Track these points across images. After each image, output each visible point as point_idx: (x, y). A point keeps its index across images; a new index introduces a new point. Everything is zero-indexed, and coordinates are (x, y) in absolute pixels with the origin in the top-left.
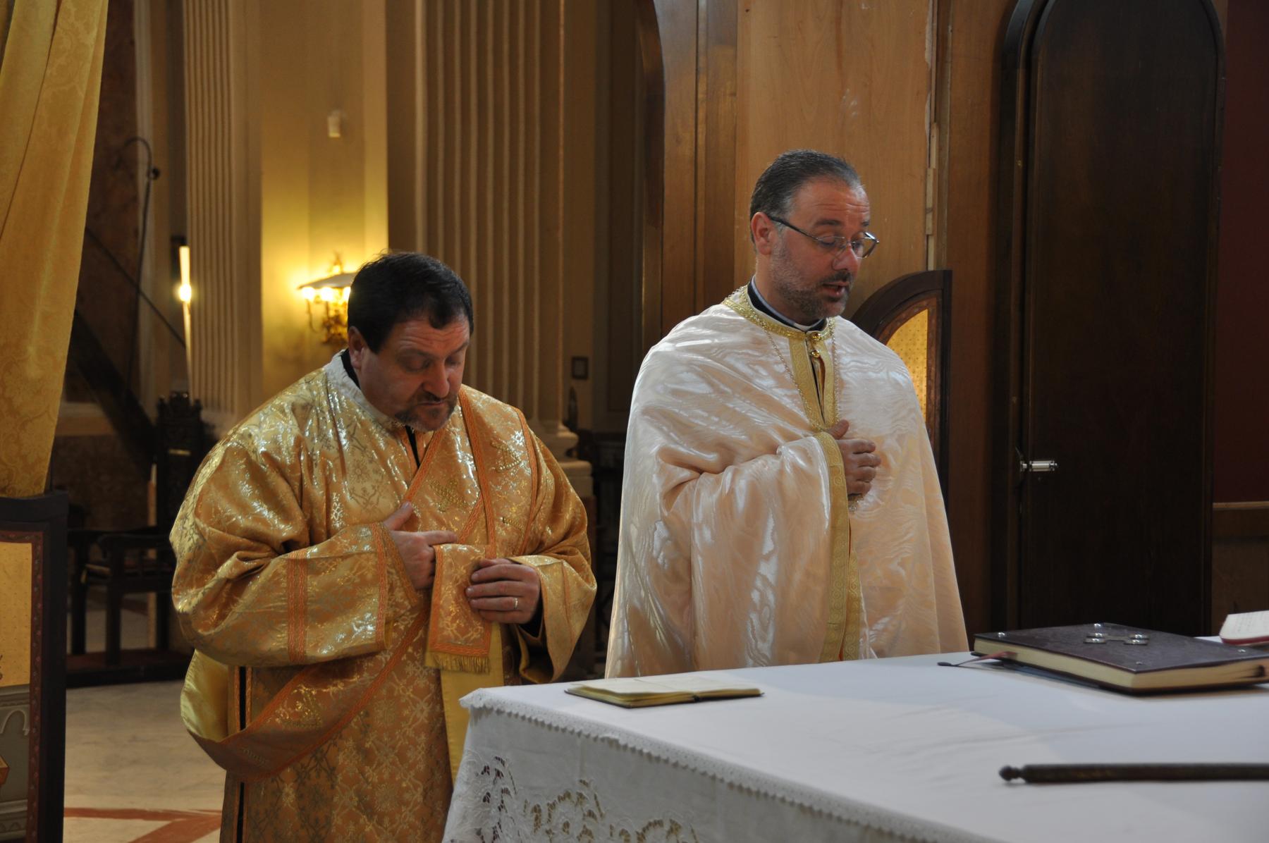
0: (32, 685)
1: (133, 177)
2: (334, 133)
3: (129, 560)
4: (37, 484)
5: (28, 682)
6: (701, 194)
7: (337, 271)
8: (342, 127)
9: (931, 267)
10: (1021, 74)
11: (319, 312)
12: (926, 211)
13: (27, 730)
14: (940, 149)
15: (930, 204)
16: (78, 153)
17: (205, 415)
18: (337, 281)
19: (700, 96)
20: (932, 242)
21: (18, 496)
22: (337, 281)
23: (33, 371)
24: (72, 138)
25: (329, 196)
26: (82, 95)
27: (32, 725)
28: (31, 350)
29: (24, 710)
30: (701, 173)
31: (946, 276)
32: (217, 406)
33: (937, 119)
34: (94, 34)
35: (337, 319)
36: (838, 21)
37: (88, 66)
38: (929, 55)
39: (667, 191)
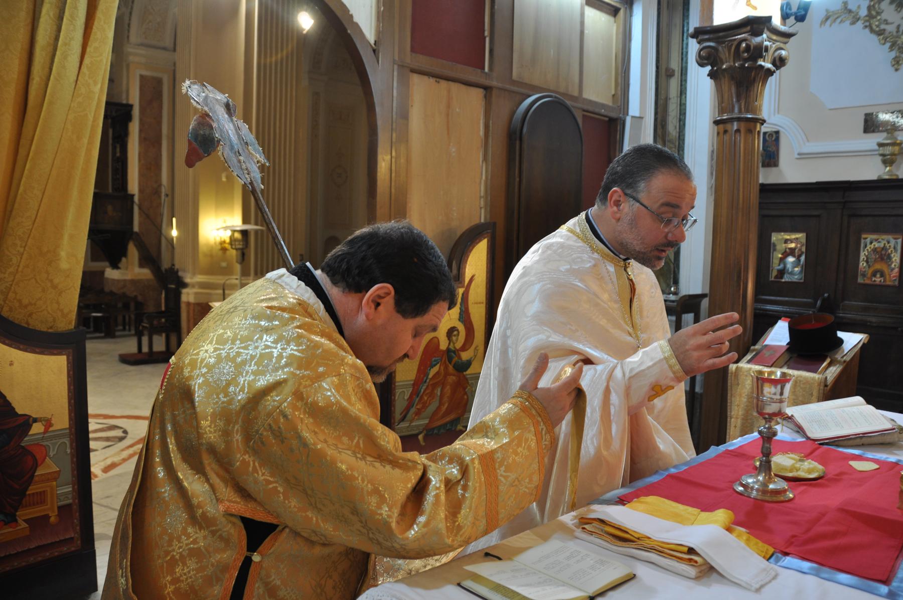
0: (70, 428)
1: (160, 197)
2: (224, 179)
3: (155, 322)
4: (70, 323)
5: (67, 426)
6: (393, 184)
7: (224, 225)
8: (227, 177)
9: (482, 221)
10: (518, 142)
11: (218, 240)
12: (481, 197)
13: (69, 451)
14: (486, 172)
15: (482, 194)
16: (89, 151)
17: (180, 274)
18: (226, 228)
19: (394, 140)
20: (483, 211)
21: (60, 330)
22: (226, 228)
23: (64, 265)
24: (85, 141)
25: (222, 201)
26: (91, 117)
27: (71, 448)
28: (63, 254)
29: (67, 441)
30: (393, 175)
31: (495, 224)
32: (184, 271)
33: (485, 159)
34: (99, 86)
35: (224, 242)
36: (448, 115)
37: (95, 103)
38: (482, 133)
39: (379, 183)
